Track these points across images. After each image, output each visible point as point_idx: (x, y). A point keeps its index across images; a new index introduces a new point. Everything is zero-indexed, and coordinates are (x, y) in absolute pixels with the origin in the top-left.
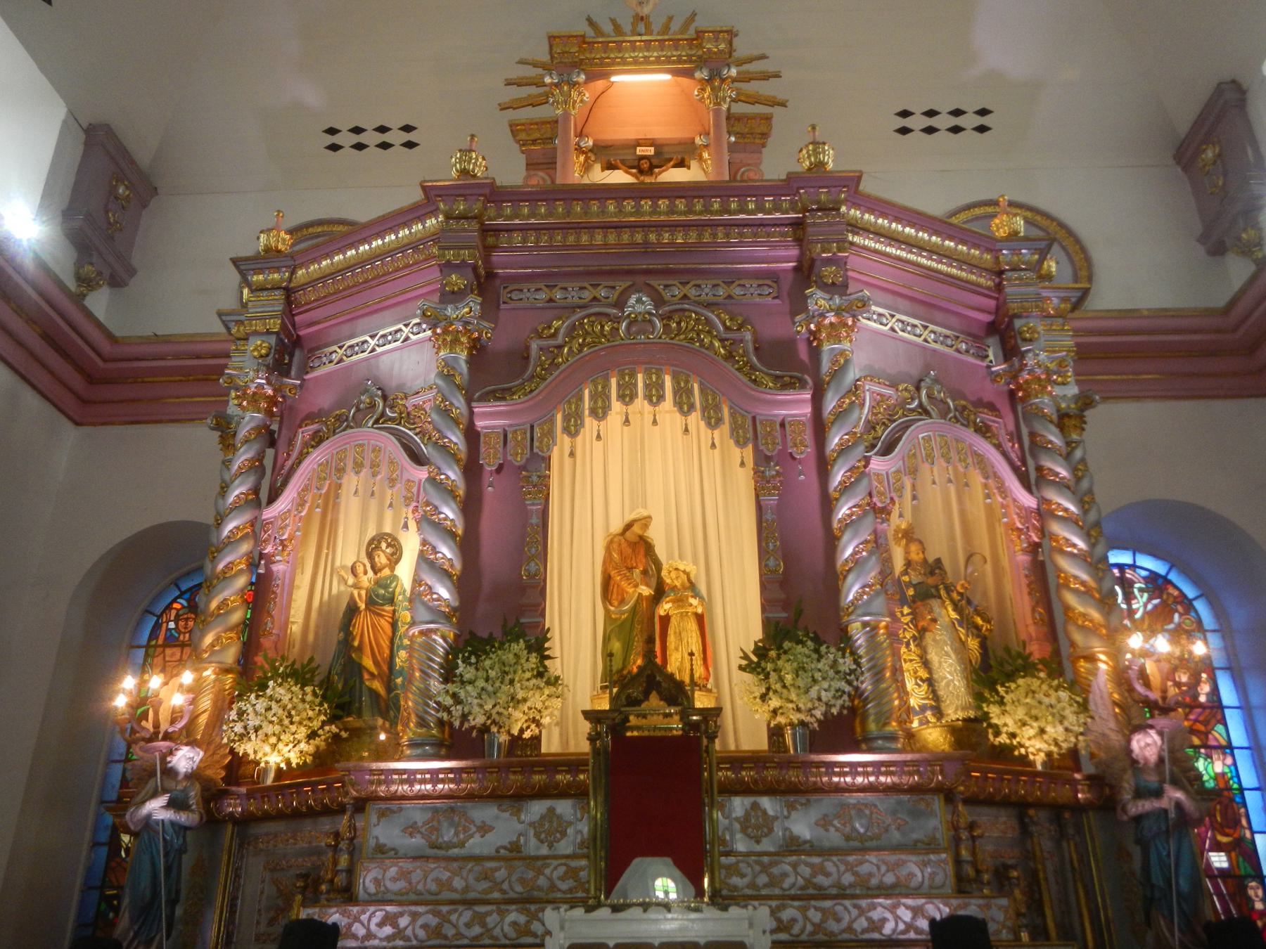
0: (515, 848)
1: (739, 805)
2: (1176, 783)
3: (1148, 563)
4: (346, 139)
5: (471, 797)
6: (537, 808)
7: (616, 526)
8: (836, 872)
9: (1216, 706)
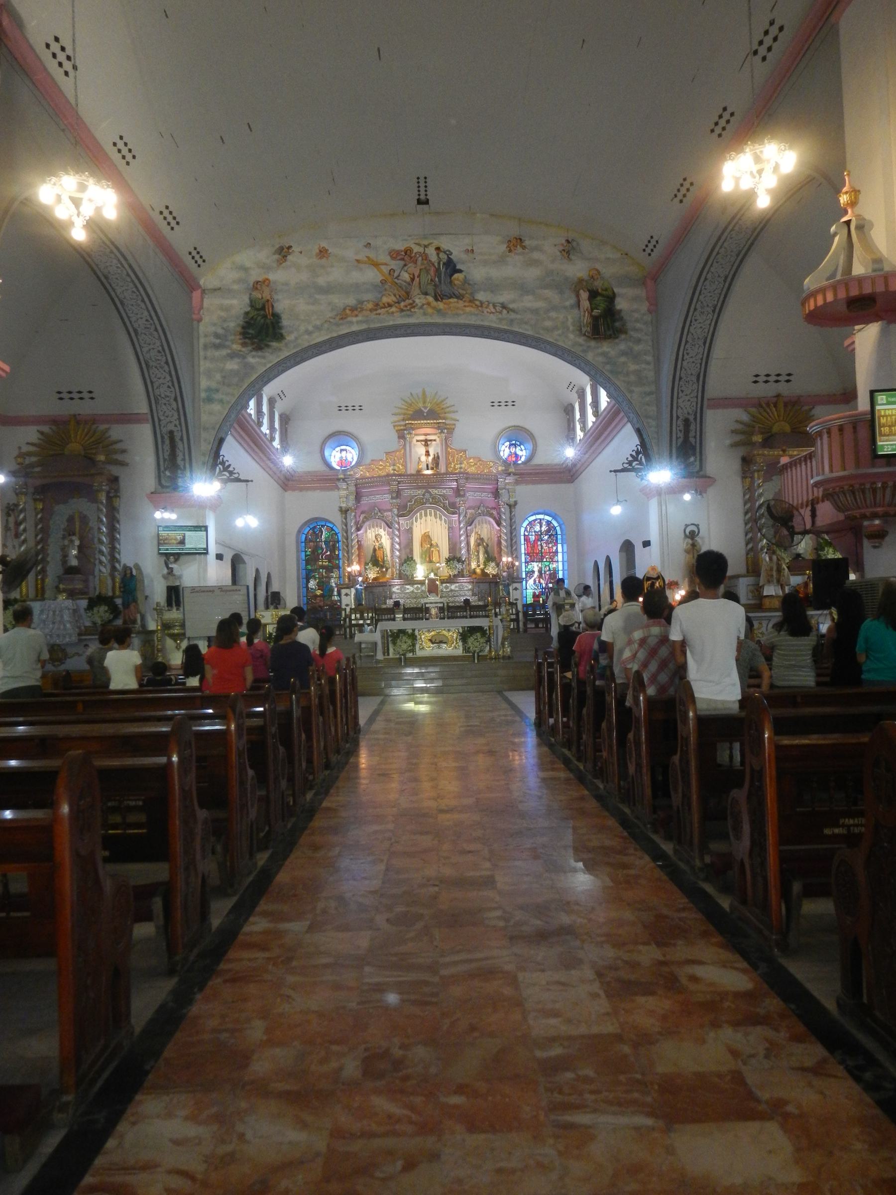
0: (413, 592)
1: (444, 585)
2: (508, 579)
3: (549, 518)
4: (343, 408)
5: (406, 585)
6: (416, 586)
7: (423, 533)
8: (457, 594)
9: (556, 552)
